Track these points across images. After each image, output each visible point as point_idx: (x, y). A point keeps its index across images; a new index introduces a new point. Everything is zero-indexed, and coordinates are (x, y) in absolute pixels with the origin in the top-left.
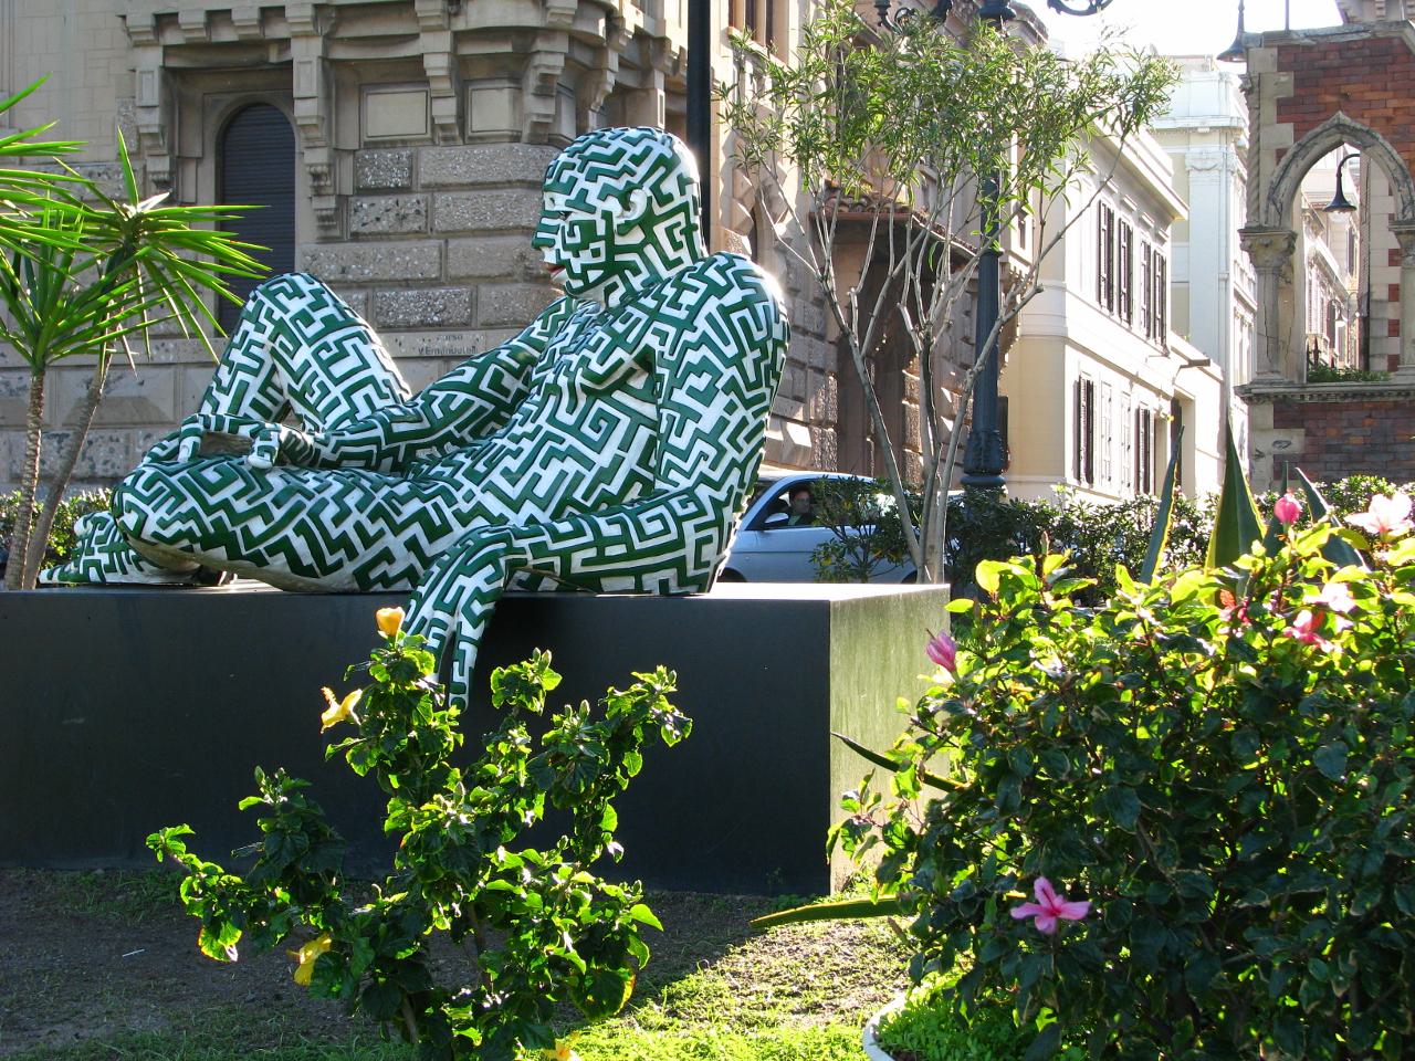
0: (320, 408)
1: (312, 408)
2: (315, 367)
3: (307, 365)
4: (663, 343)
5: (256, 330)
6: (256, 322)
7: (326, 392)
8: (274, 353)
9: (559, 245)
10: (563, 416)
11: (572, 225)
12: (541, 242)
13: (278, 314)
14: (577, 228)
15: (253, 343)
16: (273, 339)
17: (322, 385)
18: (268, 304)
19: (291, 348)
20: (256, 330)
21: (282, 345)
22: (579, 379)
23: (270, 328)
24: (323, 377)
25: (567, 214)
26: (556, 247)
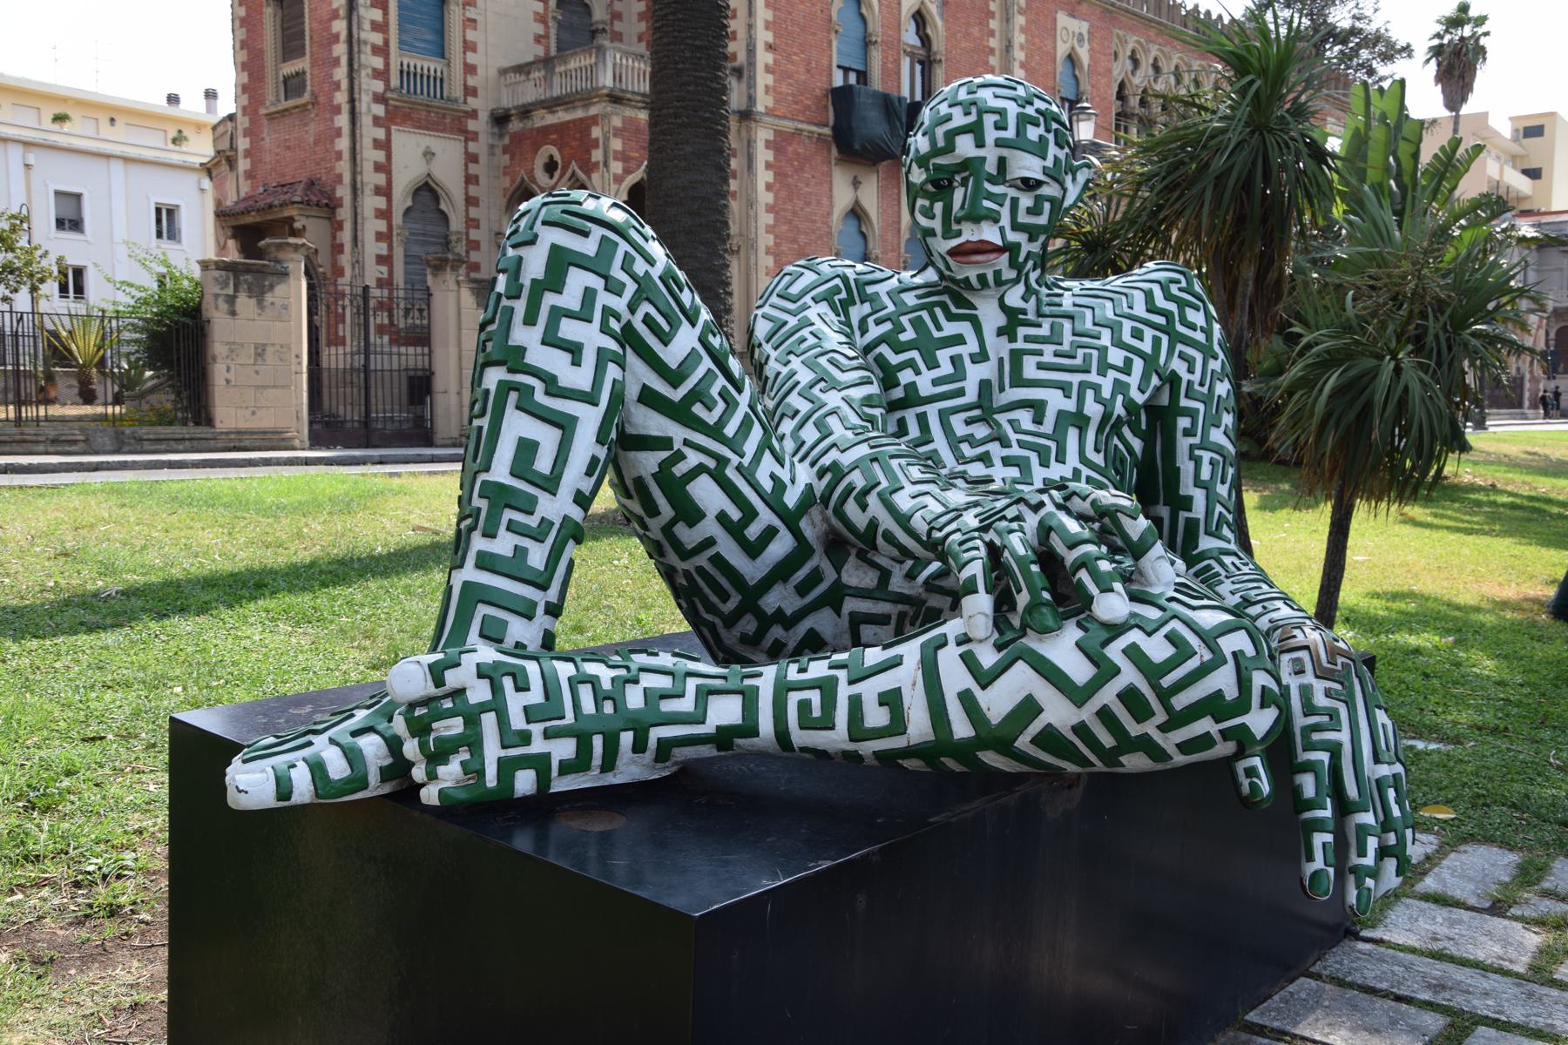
0: (730, 430)
1: (715, 432)
2: (707, 363)
3: (692, 359)
4: (1191, 371)
5: (606, 289)
6: (606, 277)
7: (731, 405)
8: (628, 328)
9: (1005, 221)
10: (1091, 454)
11: (1039, 200)
12: (985, 212)
13: (640, 267)
14: (1047, 206)
15: (608, 312)
16: (632, 308)
17: (723, 394)
18: (623, 246)
19: (666, 328)
20: (606, 289)
21: (647, 320)
22: (1119, 410)
23: (631, 287)
24: (721, 381)
25: (1039, 183)
26: (1001, 224)
